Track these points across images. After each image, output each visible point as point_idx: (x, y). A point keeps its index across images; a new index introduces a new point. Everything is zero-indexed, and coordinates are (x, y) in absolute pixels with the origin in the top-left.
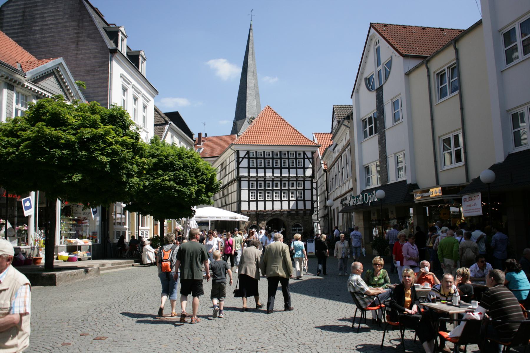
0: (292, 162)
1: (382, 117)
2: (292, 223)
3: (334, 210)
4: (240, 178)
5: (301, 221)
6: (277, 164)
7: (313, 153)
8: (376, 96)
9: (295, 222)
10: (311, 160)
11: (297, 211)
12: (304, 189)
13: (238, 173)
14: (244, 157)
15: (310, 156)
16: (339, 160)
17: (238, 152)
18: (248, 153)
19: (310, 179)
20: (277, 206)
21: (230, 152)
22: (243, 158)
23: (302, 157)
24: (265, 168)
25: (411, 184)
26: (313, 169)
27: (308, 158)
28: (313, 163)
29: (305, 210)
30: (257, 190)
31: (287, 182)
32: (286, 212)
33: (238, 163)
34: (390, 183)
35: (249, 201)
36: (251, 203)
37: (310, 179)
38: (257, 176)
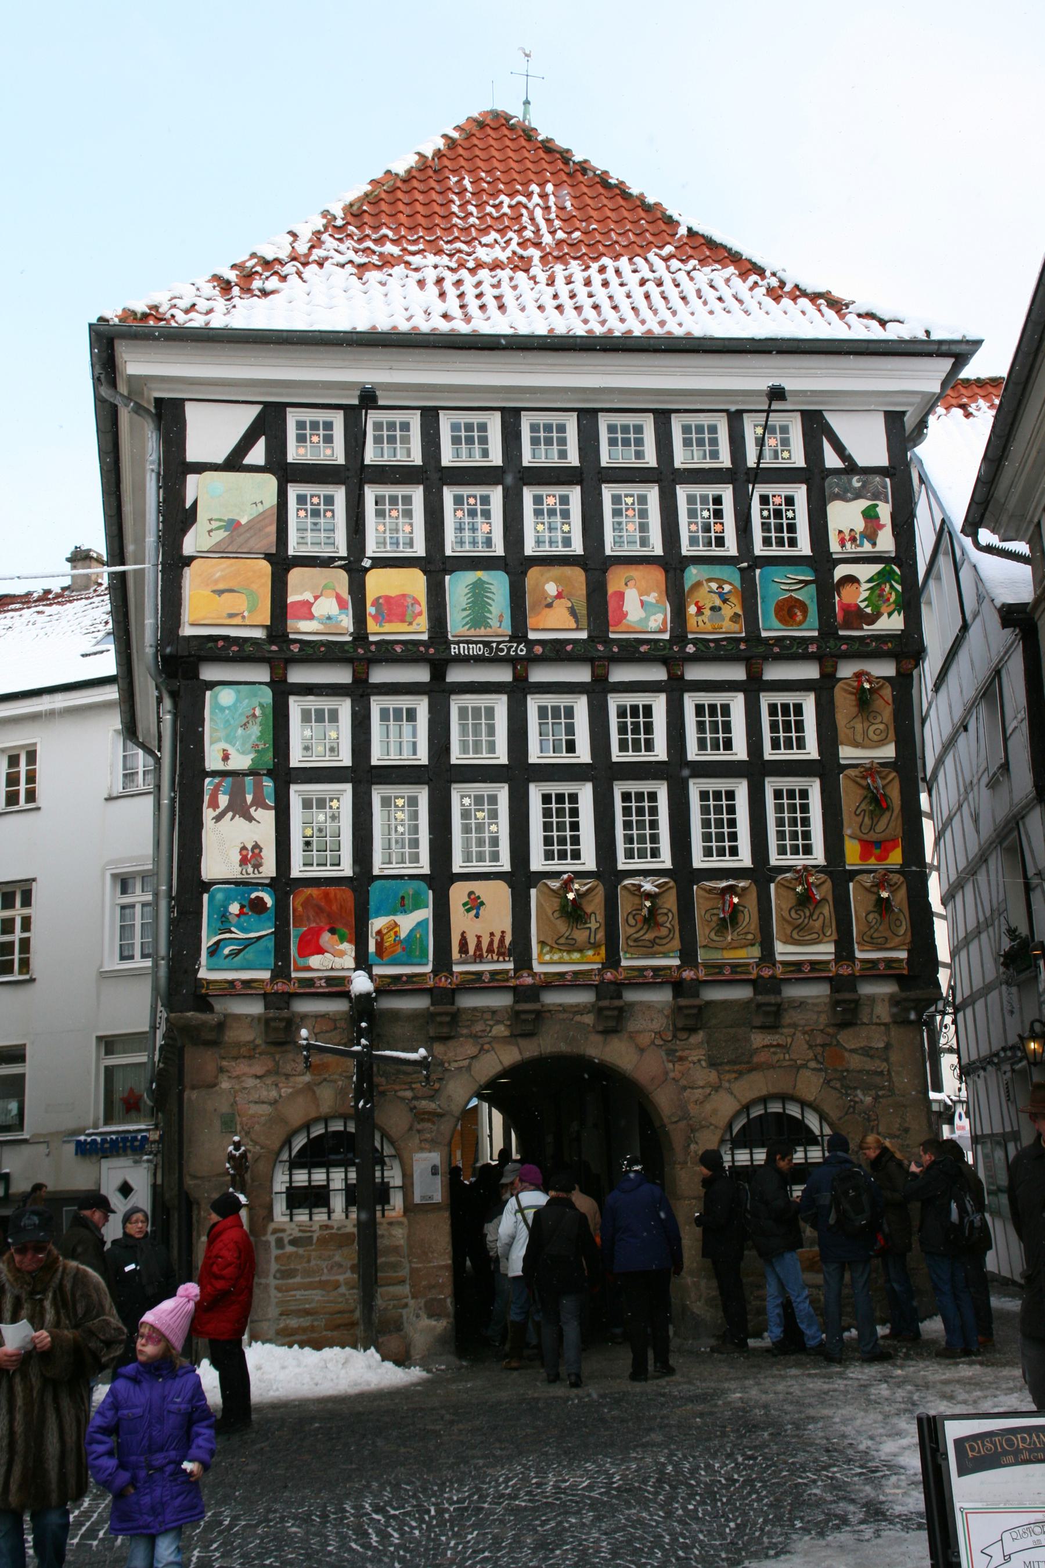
2: (724, 1106)
4: (196, 676)
5: (810, 1085)
9: (753, 1086)
18: (269, 423)
23: (799, 460)
30: (363, 775)
31: (659, 704)
32: (663, 997)
38: (360, 634)
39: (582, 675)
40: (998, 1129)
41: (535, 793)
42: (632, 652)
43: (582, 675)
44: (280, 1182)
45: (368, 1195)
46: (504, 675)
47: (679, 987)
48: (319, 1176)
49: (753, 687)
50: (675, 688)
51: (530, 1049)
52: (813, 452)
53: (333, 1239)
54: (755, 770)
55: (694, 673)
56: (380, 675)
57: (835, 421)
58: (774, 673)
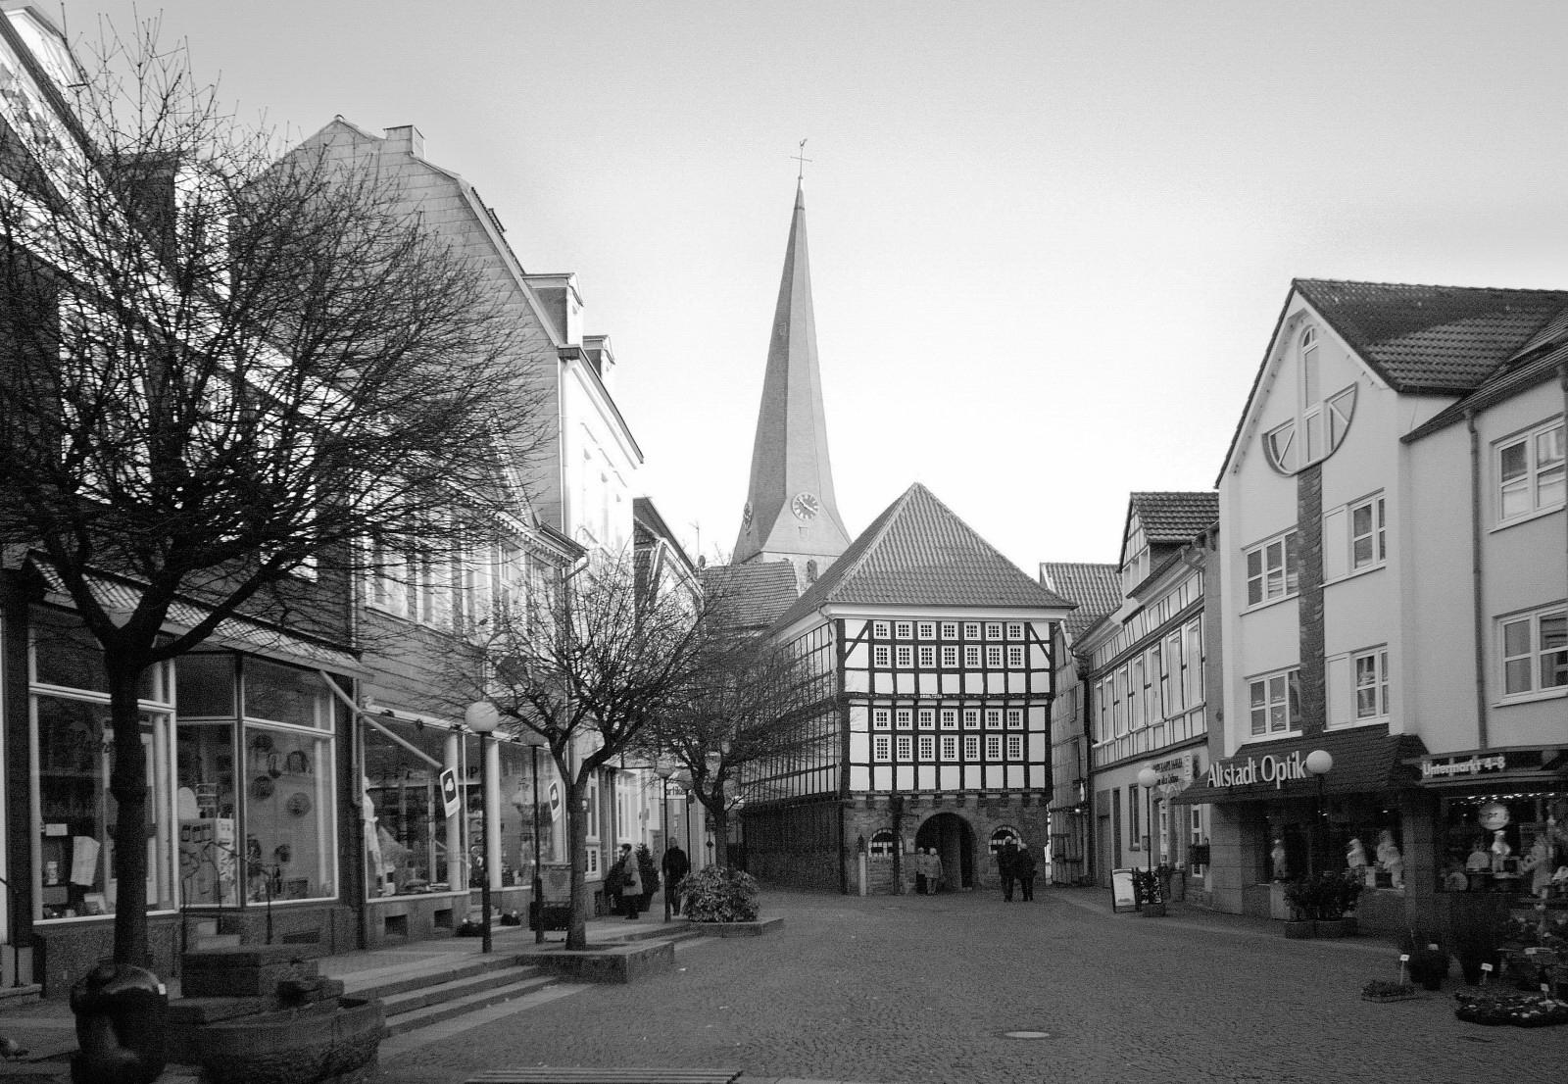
0: (995, 653)
1: (1316, 549)
3: (1117, 792)
5: (1015, 823)
6: (950, 659)
7: (1054, 626)
8: (1300, 491)
9: (1001, 822)
10: (1047, 647)
11: (1005, 793)
12: (1026, 732)
13: (842, 682)
14: (859, 640)
15: (1043, 632)
16: (1148, 652)
17: (840, 624)
18: (869, 626)
19: (1045, 702)
20: (950, 779)
21: (815, 618)
22: (856, 641)
24: (916, 671)
25: (1402, 737)
26: (1052, 672)
27: (1040, 642)
28: (1051, 657)
29: (1026, 793)
30: (894, 733)
32: (976, 797)
33: (842, 655)
34: (1332, 728)
35: (872, 765)
36: (876, 769)
37: (1045, 702)
39: (957, 703)
40: (1061, 832)
41: (942, 738)
42: (971, 697)
43: (957, 703)
44: (870, 845)
45: (893, 850)
46: (935, 703)
47: (981, 795)
48: (880, 844)
49: (1005, 707)
50: (983, 707)
51: (939, 811)
52: (1027, 635)
53: (884, 861)
54: (1005, 732)
55: (988, 703)
56: (899, 703)
57: (1034, 626)
58: (1011, 703)
